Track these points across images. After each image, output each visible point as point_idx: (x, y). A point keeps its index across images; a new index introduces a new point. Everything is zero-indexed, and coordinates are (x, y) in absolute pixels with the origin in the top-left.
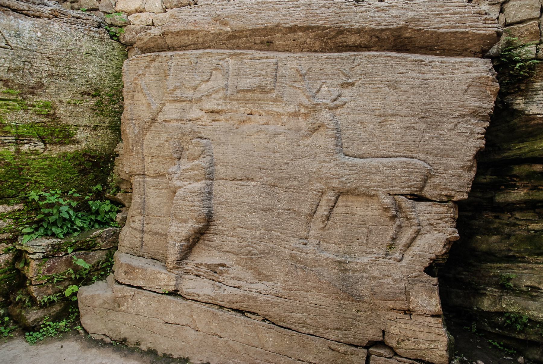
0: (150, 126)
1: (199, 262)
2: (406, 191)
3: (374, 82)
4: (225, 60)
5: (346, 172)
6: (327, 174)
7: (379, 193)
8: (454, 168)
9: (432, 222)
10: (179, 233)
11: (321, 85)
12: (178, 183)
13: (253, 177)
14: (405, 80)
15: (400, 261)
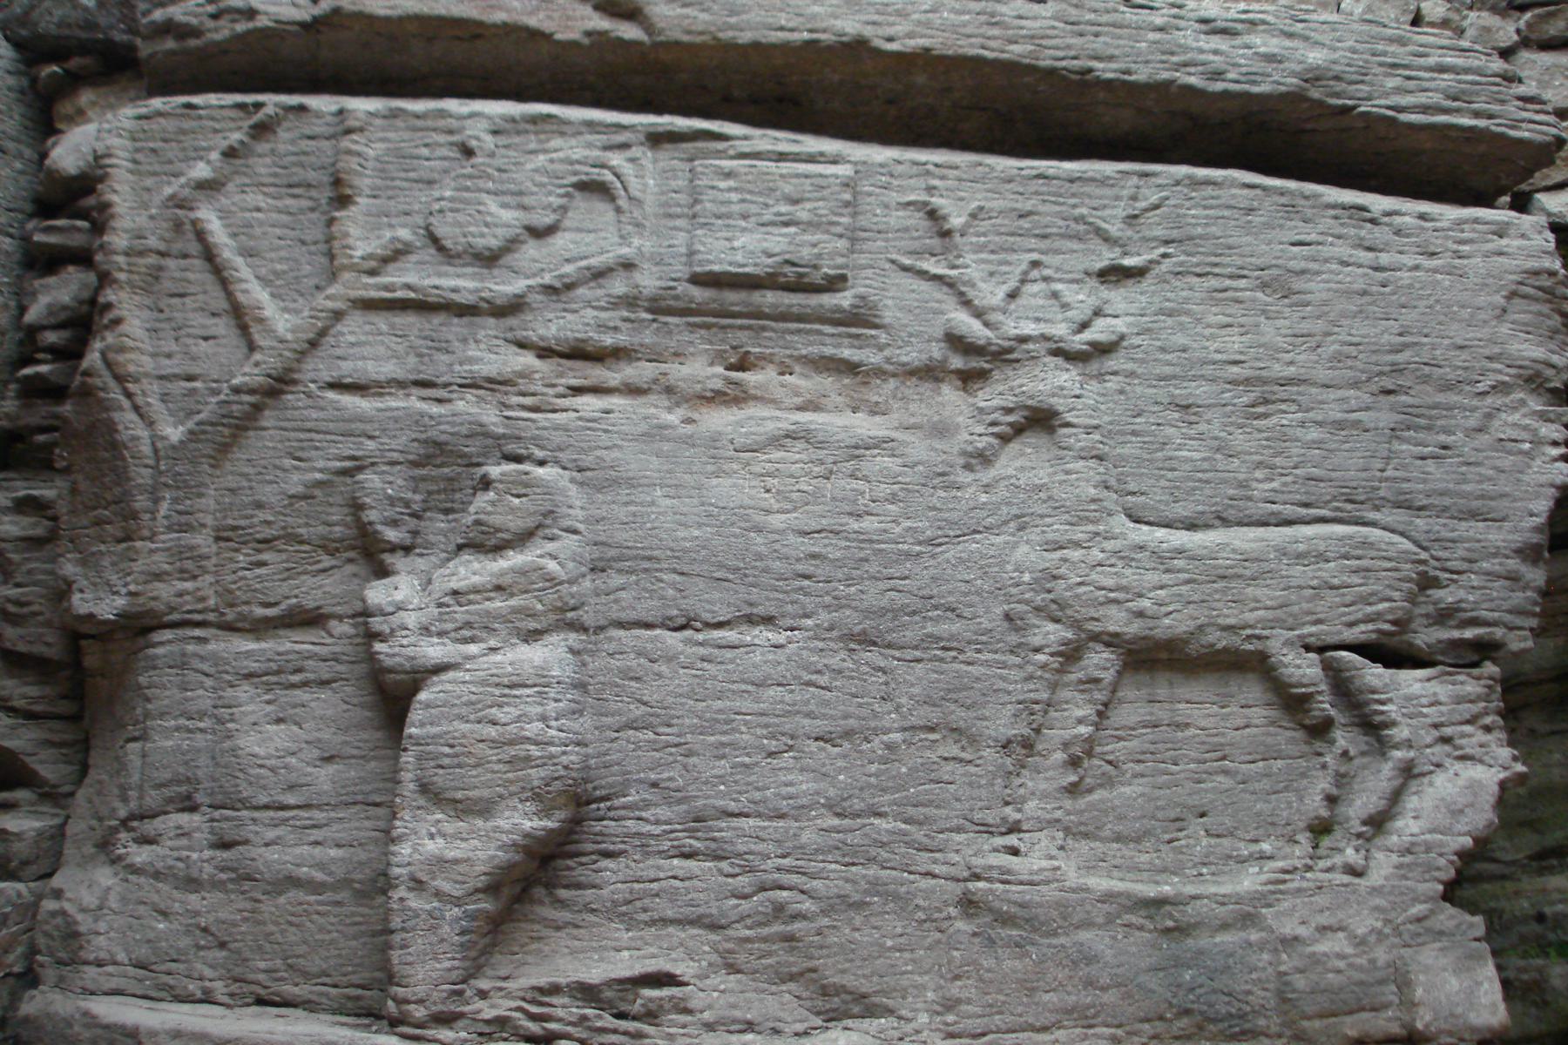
0: (257, 408)
1: (543, 981)
3: (1217, 270)
5: (1153, 578)
8: (1495, 555)
9: (1448, 731)
10: (456, 861)
11: (1025, 273)
12: (434, 651)
13: (773, 611)
14: (1314, 266)
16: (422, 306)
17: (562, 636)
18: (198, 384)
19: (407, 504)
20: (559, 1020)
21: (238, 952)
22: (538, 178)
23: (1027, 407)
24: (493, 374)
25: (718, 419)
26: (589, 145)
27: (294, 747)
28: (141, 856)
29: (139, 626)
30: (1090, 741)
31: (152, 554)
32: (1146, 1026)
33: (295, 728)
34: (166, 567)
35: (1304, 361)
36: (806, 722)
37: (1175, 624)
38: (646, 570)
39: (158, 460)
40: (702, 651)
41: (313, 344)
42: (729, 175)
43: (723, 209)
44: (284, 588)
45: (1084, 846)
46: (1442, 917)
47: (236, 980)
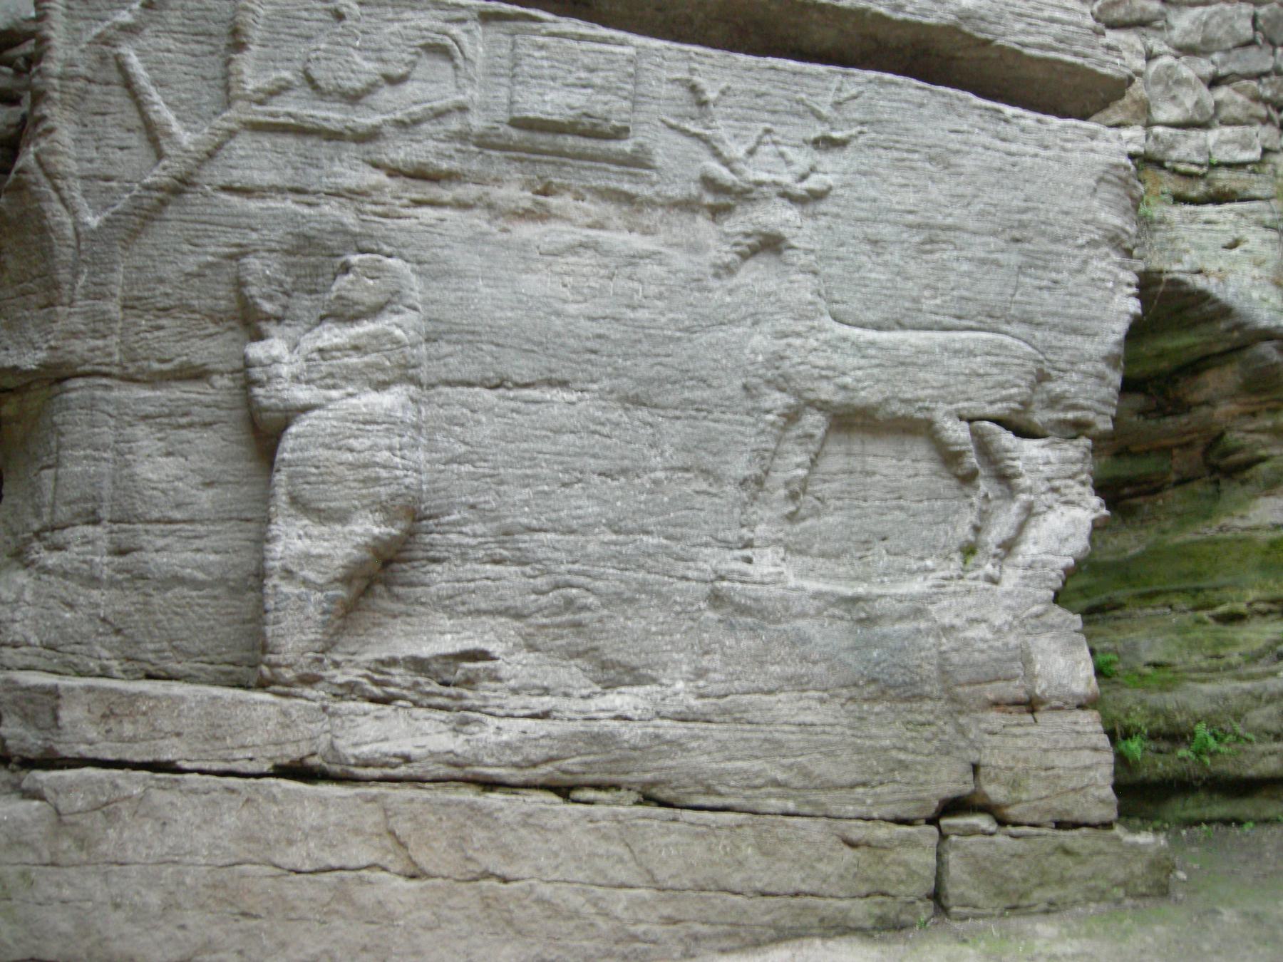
0: (163, 203)
2: (997, 409)
4: (465, 27)
6: (801, 368)
7: (938, 416)
9: (1057, 483)
10: (320, 556)
11: (760, 137)
12: (302, 394)
13: (567, 377)
14: (966, 148)
16: (300, 130)
18: (114, 184)
20: (397, 685)
21: (132, 636)
22: (394, 39)
23: (761, 234)
24: (353, 186)
25: (526, 231)
26: (435, 18)
27: (181, 473)
28: (52, 559)
29: (56, 376)
30: (805, 481)
31: (70, 317)
32: (844, 691)
33: (182, 460)
34: (82, 327)
35: (957, 214)
36: (592, 461)
37: (869, 395)
38: (470, 342)
39: (79, 242)
40: (512, 404)
41: (211, 155)
42: (541, 47)
43: (537, 72)
44: (178, 348)
45: (799, 560)
47: (128, 659)
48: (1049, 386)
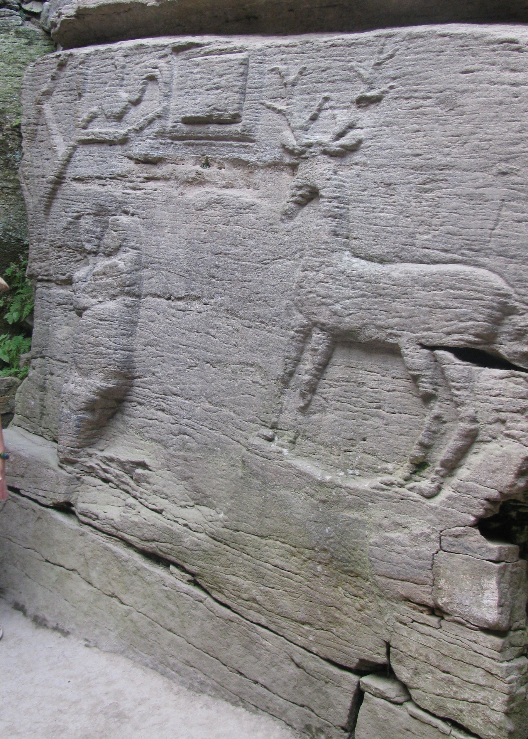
2: (452, 340)
4: (167, 59)
6: (312, 295)
7: (402, 342)
9: (503, 415)
11: (320, 105)
14: (472, 86)
15: (430, 497)
17: (123, 298)
19: (94, 232)
23: (308, 186)
24: (120, 173)
25: (193, 194)
32: (307, 551)
37: (349, 322)
41: (68, 161)
46: (471, 539)
48: (516, 318)
